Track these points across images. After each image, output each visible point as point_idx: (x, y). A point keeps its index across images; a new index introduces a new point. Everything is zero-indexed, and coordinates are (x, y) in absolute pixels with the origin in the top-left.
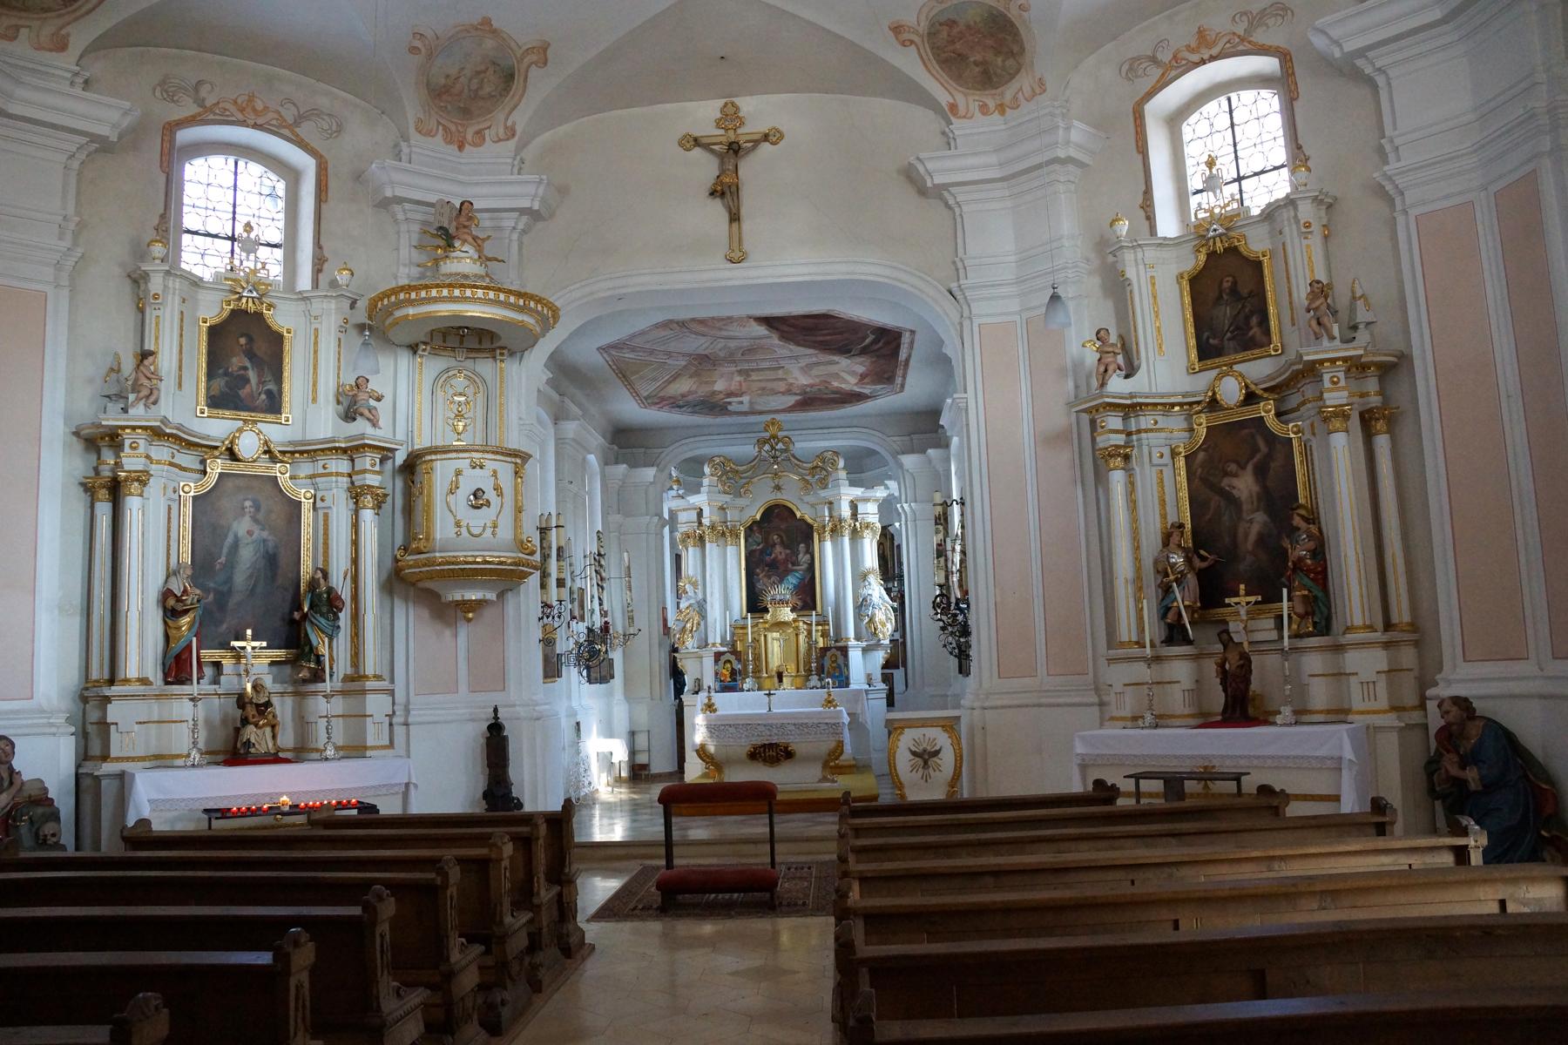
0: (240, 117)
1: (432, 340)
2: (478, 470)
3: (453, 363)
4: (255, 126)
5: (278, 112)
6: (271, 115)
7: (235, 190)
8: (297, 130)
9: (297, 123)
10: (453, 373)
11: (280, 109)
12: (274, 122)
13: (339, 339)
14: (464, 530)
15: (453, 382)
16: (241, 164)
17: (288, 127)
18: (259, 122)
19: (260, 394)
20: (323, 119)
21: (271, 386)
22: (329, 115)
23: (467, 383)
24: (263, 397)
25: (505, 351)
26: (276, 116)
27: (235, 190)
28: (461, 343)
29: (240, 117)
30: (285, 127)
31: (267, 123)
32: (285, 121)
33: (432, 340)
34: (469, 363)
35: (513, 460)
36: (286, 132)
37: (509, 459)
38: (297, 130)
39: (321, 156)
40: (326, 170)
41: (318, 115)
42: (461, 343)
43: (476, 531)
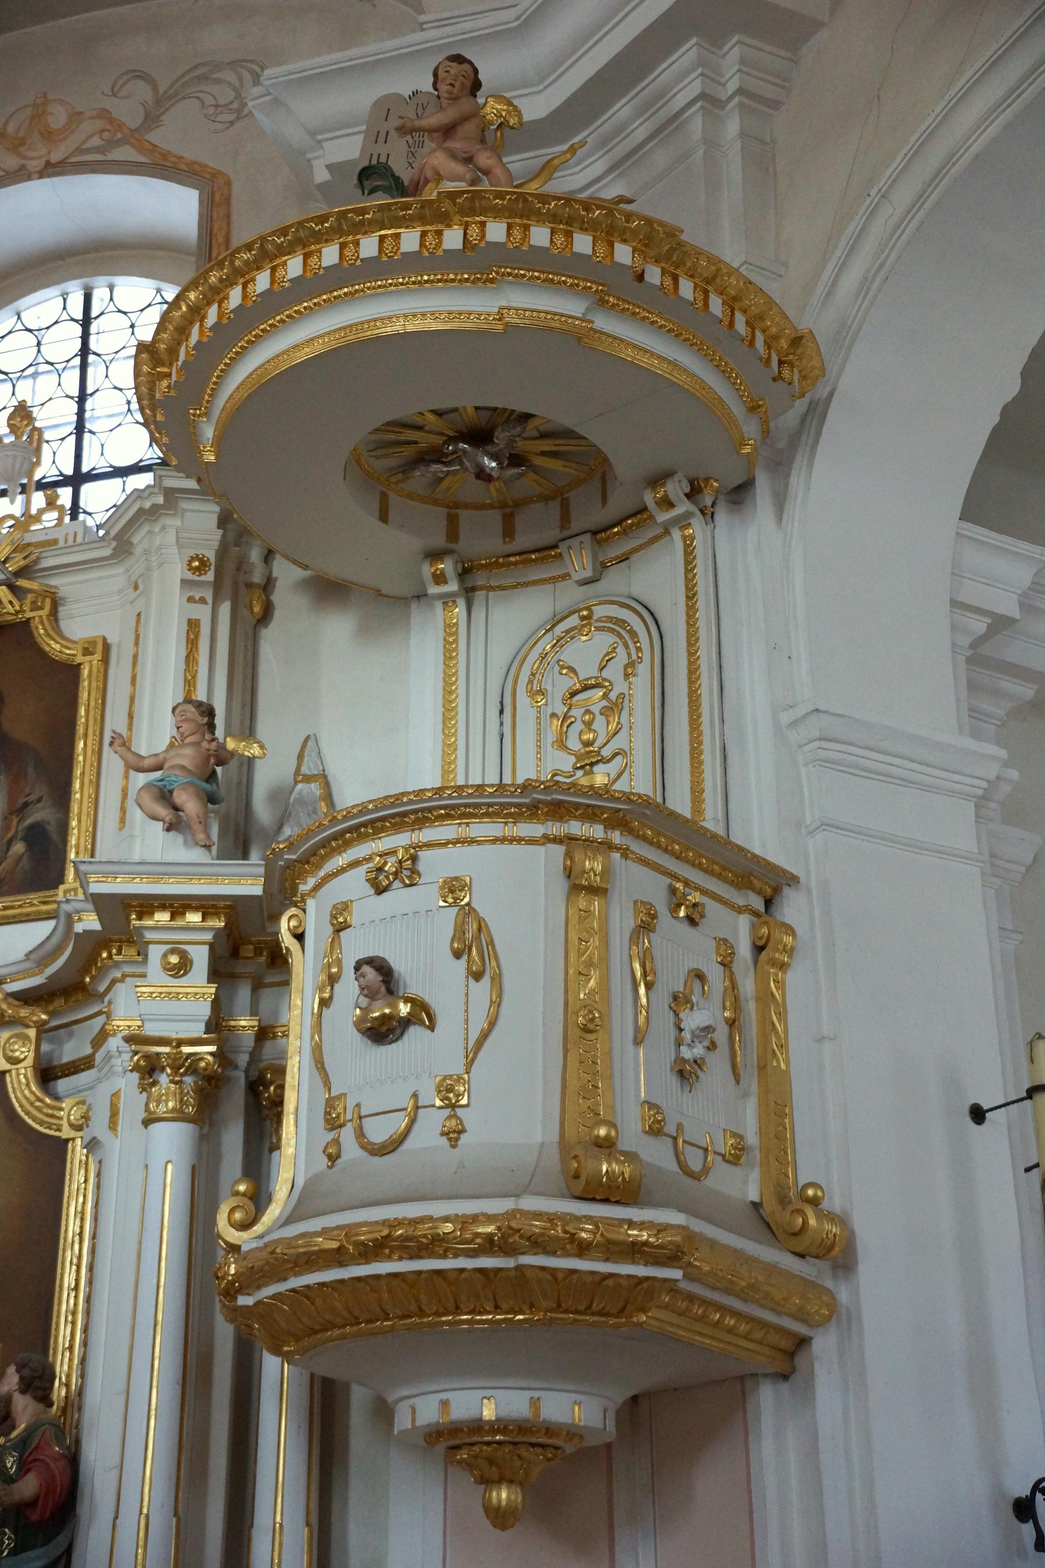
0: (12, 162)
1: (453, 534)
2: (398, 897)
3: (569, 595)
4: (51, 169)
5: (104, 114)
6: (88, 127)
7: (84, 367)
8: (154, 137)
9: (151, 119)
10: (573, 621)
11: (110, 104)
12: (96, 141)
13: (193, 625)
14: (347, 1135)
15: (569, 654)
16: (100, 296)
17: (134, 137)
18: (55, 157)
19: (10, 843)
20: (219, 81)
21: (42, 814)
22: (234, 64)
23: (610, 639)
24: (19, 848)
25: (675, 489)
26: (99, 124)
27: (84, 367)
28: (565, 518)
29: (12, 162)
30: (119, 143)
31: (79, 150)
32: (121, 126)
33: (453, 534)
34: (614, 582)
35: (555, 828)
36: (125, 153)
37: (536, 829)
38: (154, 137)
39: (215, 174)
40: (228, 201)
41: (205, 78)
42: (565, 518)
43: (379, 1131)
